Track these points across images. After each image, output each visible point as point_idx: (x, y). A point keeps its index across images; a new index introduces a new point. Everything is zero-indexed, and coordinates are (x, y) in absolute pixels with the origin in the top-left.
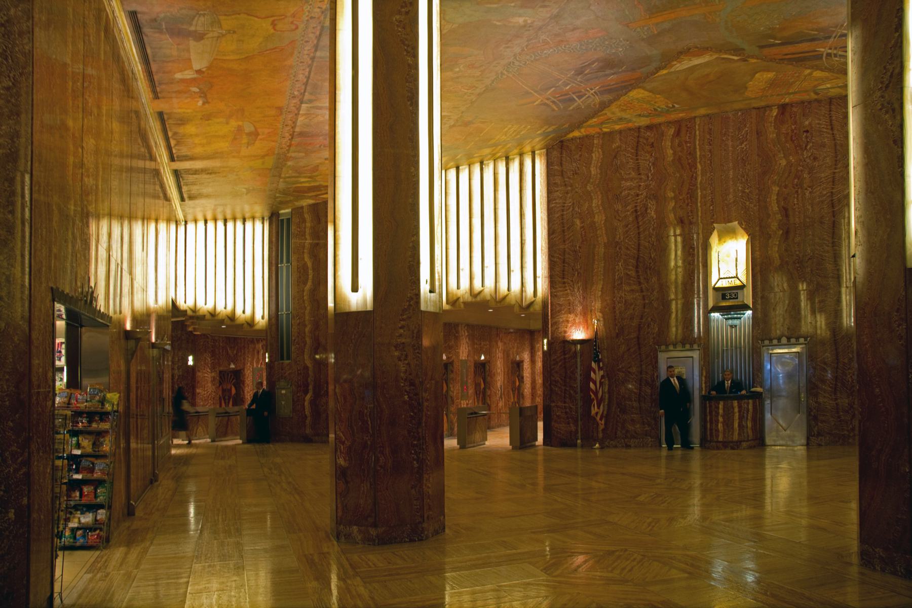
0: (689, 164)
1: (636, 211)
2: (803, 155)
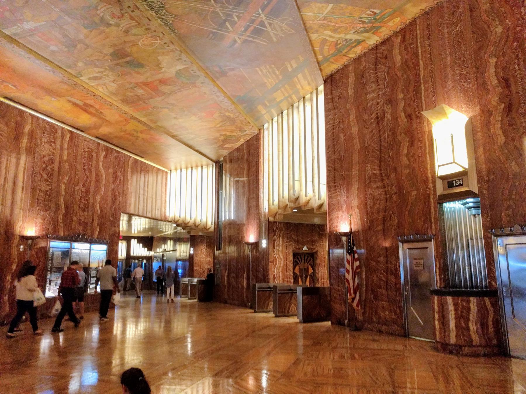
0: (413, 63)
1: (377, 118)
2: (520, 13)
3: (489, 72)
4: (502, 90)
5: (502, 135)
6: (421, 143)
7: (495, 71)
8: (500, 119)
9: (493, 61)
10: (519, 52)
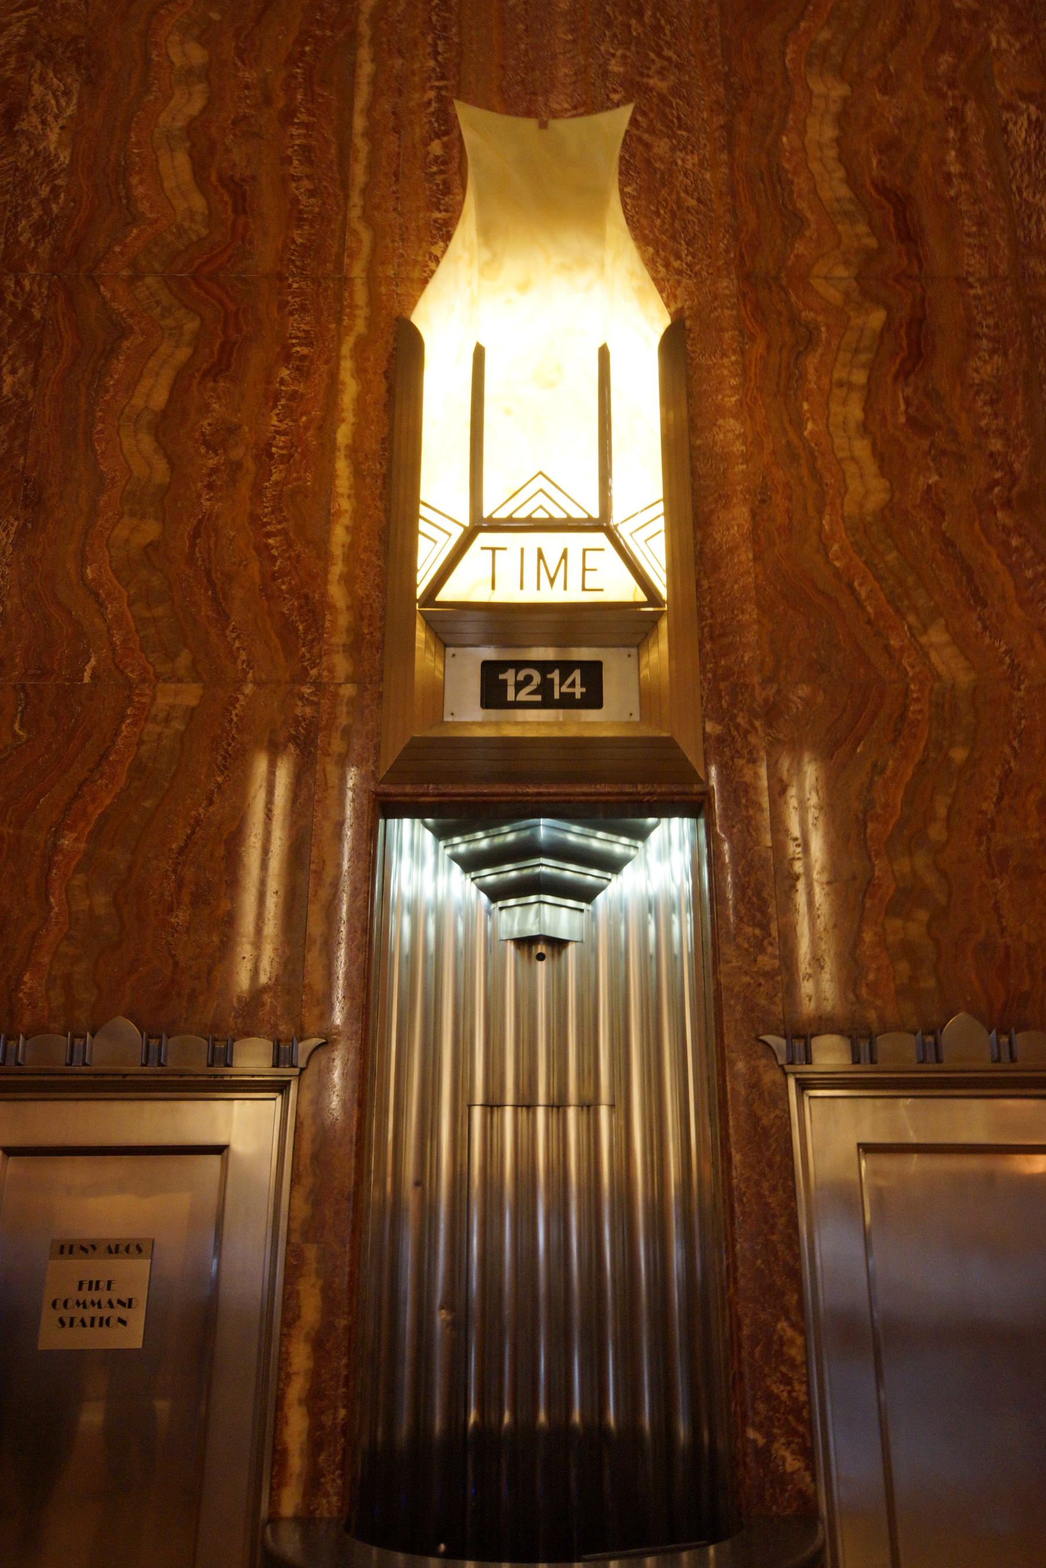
3: (802, 133)
4: (872, 243)
5: (871, 467)
6: (303, 372)
7: (838, 140)
8: (860, 377)
9: (828, 90)
10: (965, 99)
